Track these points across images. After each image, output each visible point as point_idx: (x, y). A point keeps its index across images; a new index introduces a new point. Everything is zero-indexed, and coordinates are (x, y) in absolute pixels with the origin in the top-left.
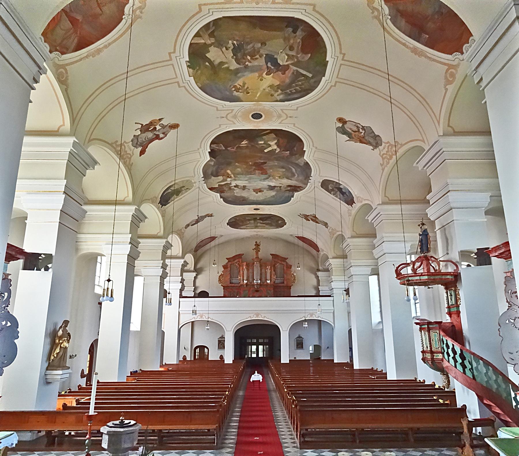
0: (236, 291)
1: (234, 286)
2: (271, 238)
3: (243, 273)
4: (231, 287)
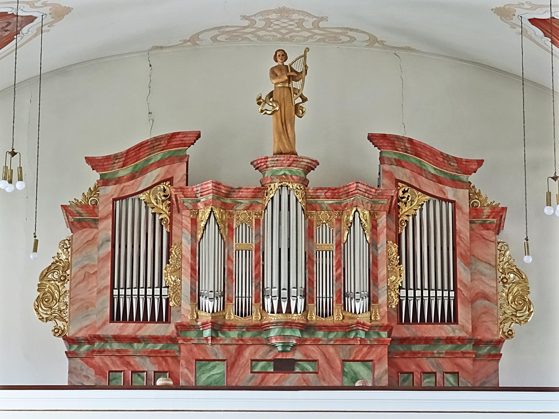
0: (149, 366)
1: (135, 339)
2: (373, 41)
4: (116, 346)
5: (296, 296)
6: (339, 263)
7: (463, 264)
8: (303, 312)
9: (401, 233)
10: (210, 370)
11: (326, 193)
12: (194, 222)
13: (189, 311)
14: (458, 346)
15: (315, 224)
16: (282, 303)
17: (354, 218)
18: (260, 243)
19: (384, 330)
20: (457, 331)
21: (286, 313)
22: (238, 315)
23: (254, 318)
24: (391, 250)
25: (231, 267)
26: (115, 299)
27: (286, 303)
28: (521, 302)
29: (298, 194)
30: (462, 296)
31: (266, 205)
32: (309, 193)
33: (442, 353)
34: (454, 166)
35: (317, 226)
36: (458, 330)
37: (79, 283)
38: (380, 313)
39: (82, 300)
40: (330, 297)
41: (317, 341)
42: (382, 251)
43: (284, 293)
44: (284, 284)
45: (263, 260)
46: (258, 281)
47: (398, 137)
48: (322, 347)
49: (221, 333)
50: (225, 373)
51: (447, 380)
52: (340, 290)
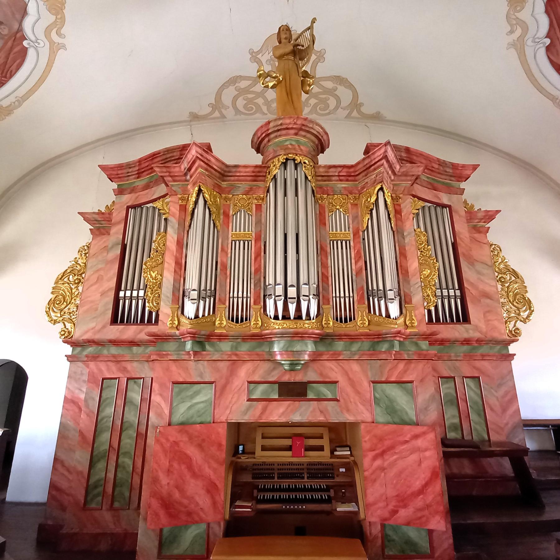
1: (132, 343)
3: (181, 244)
4: (114, 350)
5: (308, 295)
6: (358, 253)
8: (317, 317)
10: (192, 397)
11: (340, 172)
12: (183, 208)
13: (169, 316)
15: (327, 210)
16: (290, 305)
17: (377, 199)
18: (261, 231)
19: (425, 339)
21: (294, 318)
22: (233, 320)
23: (252, 324)
24: (420, 239)
25: (225, 260)
26: (121, 301)
27: (295, 304)
28: (522, 301)
29: (307, 170)
30: (471, 294)
31: (268, 186)
32: (320, 172)
35: (330, 212)
37: (92, 285)
38: (415, 316)
39: (92, 302)
40: (349, 297)
41: (336, 356)
42: (410, 239)
43: (292, 292)
44: (292, 280)
45: (265, 253)
46: (258, 277)
49: (209, 345)
50: (212, 402)
52: (363, 287)
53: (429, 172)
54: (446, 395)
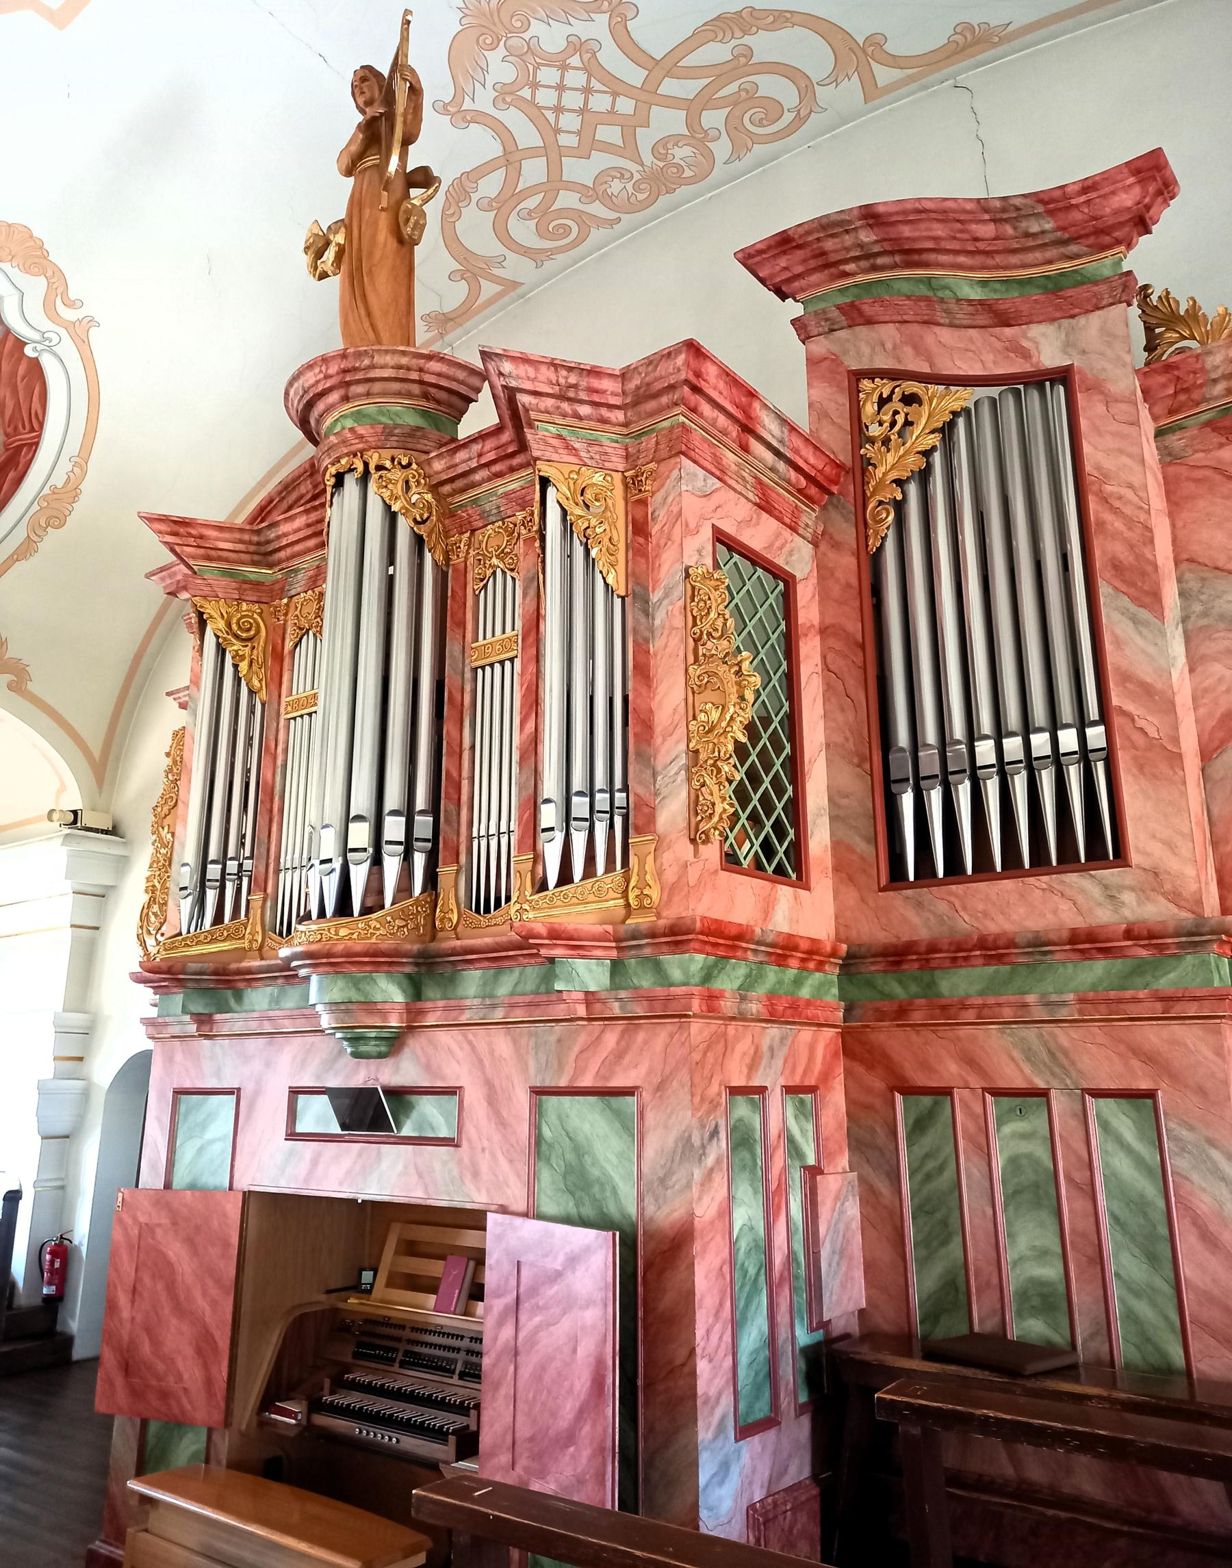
7: (1125, 602)
9: (881, 549)
11: (480, 455)
14: (1140, 969)
20: (1128, 897)
21: (361, 914)
32: (438, 473)
33: (1063, 1004)
34: (1043, 232)
36: (1132, 889)
47: (824, 221)
48: (475, 1035)
51: (1105, 1126)
53: (978, 260)
54: (1014, 1163)
